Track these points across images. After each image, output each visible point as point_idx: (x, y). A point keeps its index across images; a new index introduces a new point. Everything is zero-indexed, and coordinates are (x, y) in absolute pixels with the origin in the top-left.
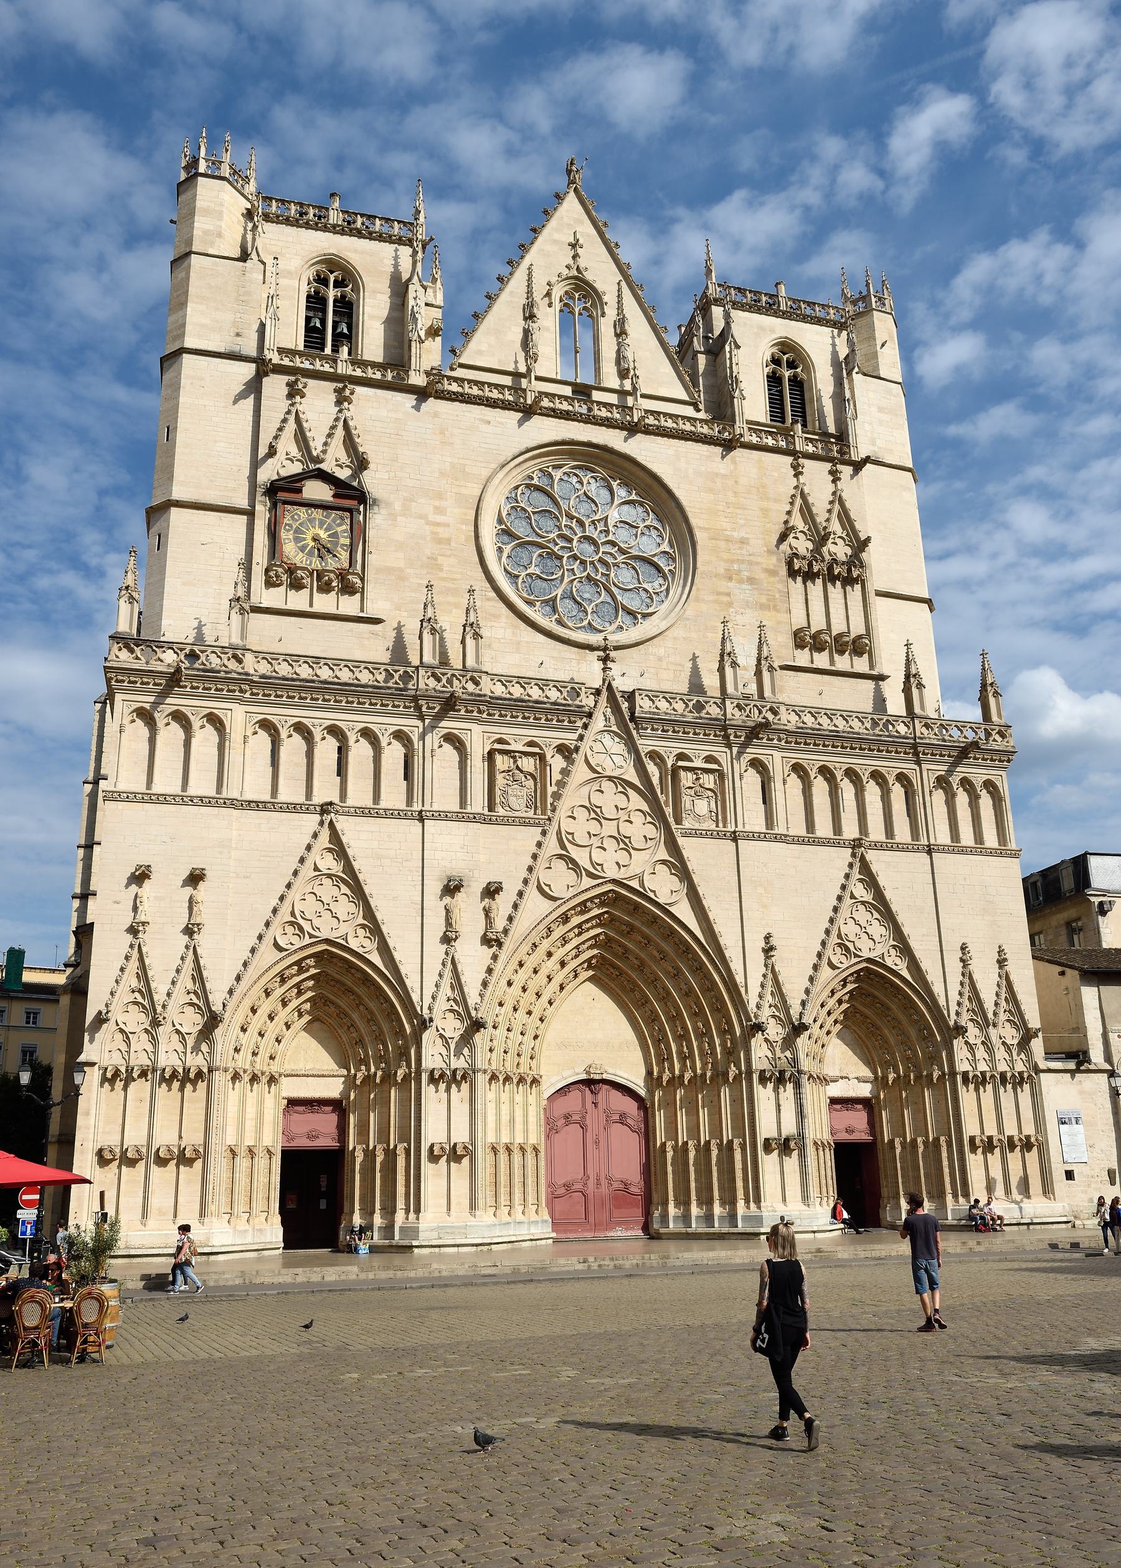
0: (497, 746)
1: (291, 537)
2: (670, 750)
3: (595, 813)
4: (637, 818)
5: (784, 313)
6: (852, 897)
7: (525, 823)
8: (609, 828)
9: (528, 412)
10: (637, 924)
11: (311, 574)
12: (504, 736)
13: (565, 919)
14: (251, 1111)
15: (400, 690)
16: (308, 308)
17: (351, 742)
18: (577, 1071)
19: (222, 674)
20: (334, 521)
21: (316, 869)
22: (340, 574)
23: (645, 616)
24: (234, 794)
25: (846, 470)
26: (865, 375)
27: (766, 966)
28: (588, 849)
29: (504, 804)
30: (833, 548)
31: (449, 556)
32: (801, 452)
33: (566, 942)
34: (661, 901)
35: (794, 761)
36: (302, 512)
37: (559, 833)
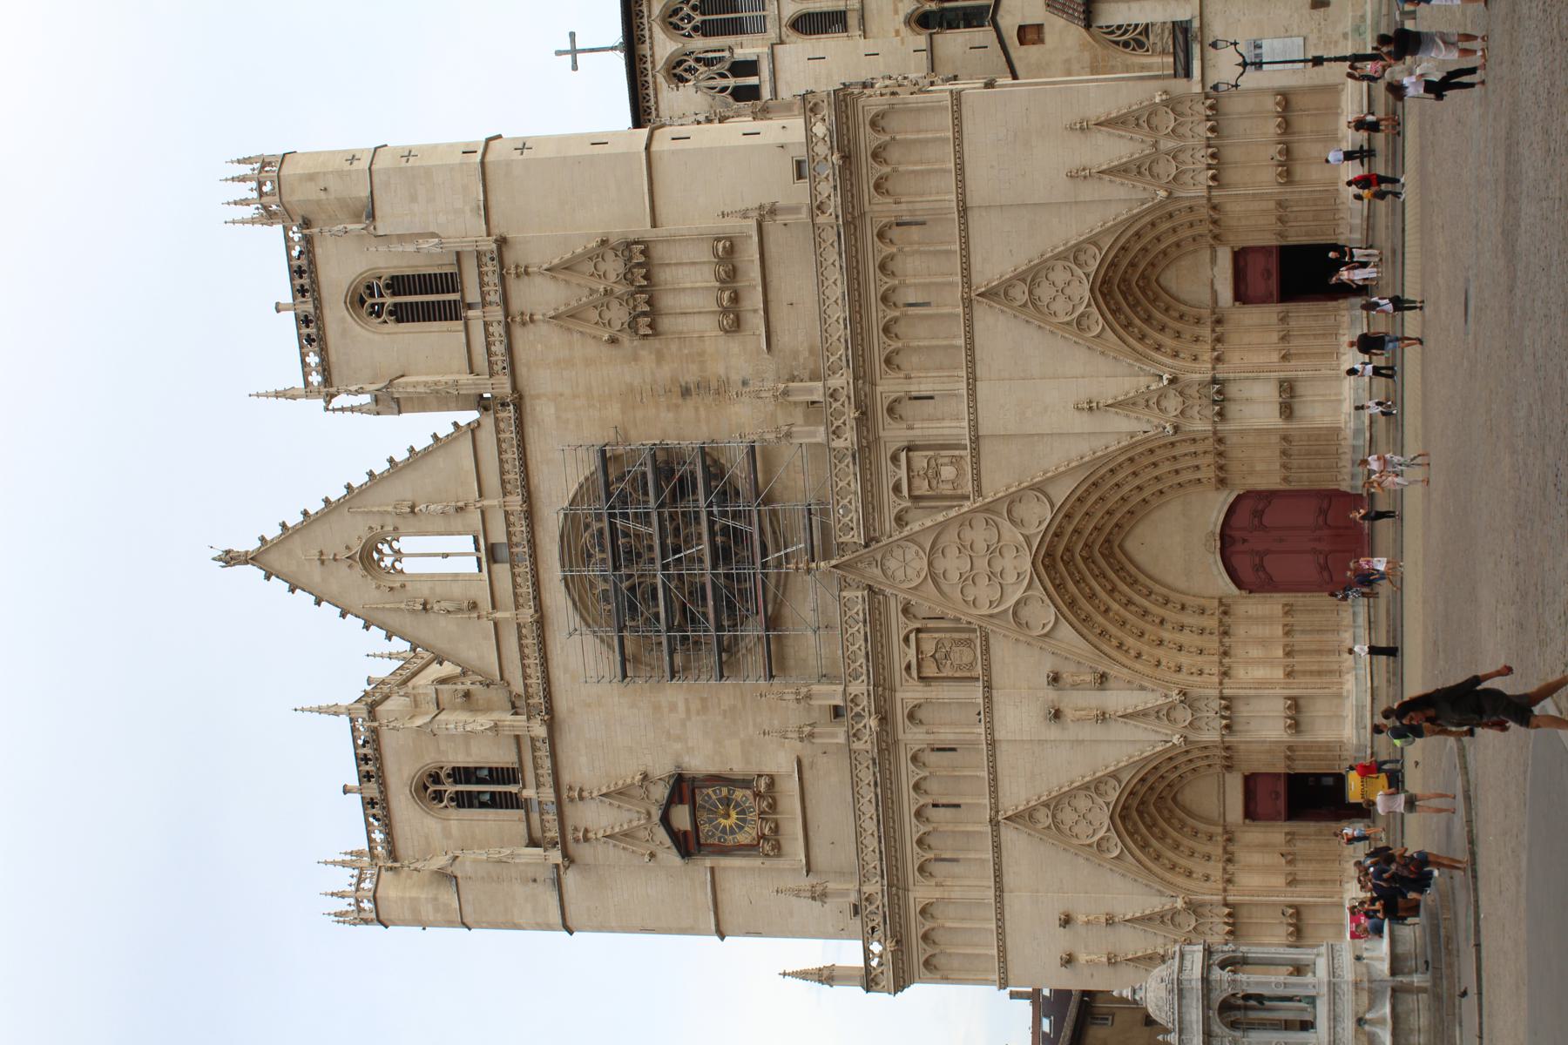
0: (914, 673)
1: (731, 837)
2: (891, 505)
3: (970, 579)
4: (968, 535)
5: (316, 308)
6: (1025, 305)
7: (986, 650)
8: (982, 564)
9: (541, 622)
10: (1071, 528)
11: (763, 819)
12: (903, 666)
13: (1072, 604)
14: (1256, 858)
15: (874, 763)
16: (471, 806)
17: (929, 800)
18: (1211, 561)
19: (886, 909)
20: (706, 802)
21: (1049, 827)
22: (758, 795)
24: (991, 894)
25: (511, 257)
26: (372, 216)
27: (1106, 411)
28: (1004, 587)
29: (971, 665)
30: (612, 277)
31: (719, 699)
32: (506, 316)
33: (1094, 595)
34: (1049, 517)
35: (883, 365)
36: (705, 829)
37: (991, 616)
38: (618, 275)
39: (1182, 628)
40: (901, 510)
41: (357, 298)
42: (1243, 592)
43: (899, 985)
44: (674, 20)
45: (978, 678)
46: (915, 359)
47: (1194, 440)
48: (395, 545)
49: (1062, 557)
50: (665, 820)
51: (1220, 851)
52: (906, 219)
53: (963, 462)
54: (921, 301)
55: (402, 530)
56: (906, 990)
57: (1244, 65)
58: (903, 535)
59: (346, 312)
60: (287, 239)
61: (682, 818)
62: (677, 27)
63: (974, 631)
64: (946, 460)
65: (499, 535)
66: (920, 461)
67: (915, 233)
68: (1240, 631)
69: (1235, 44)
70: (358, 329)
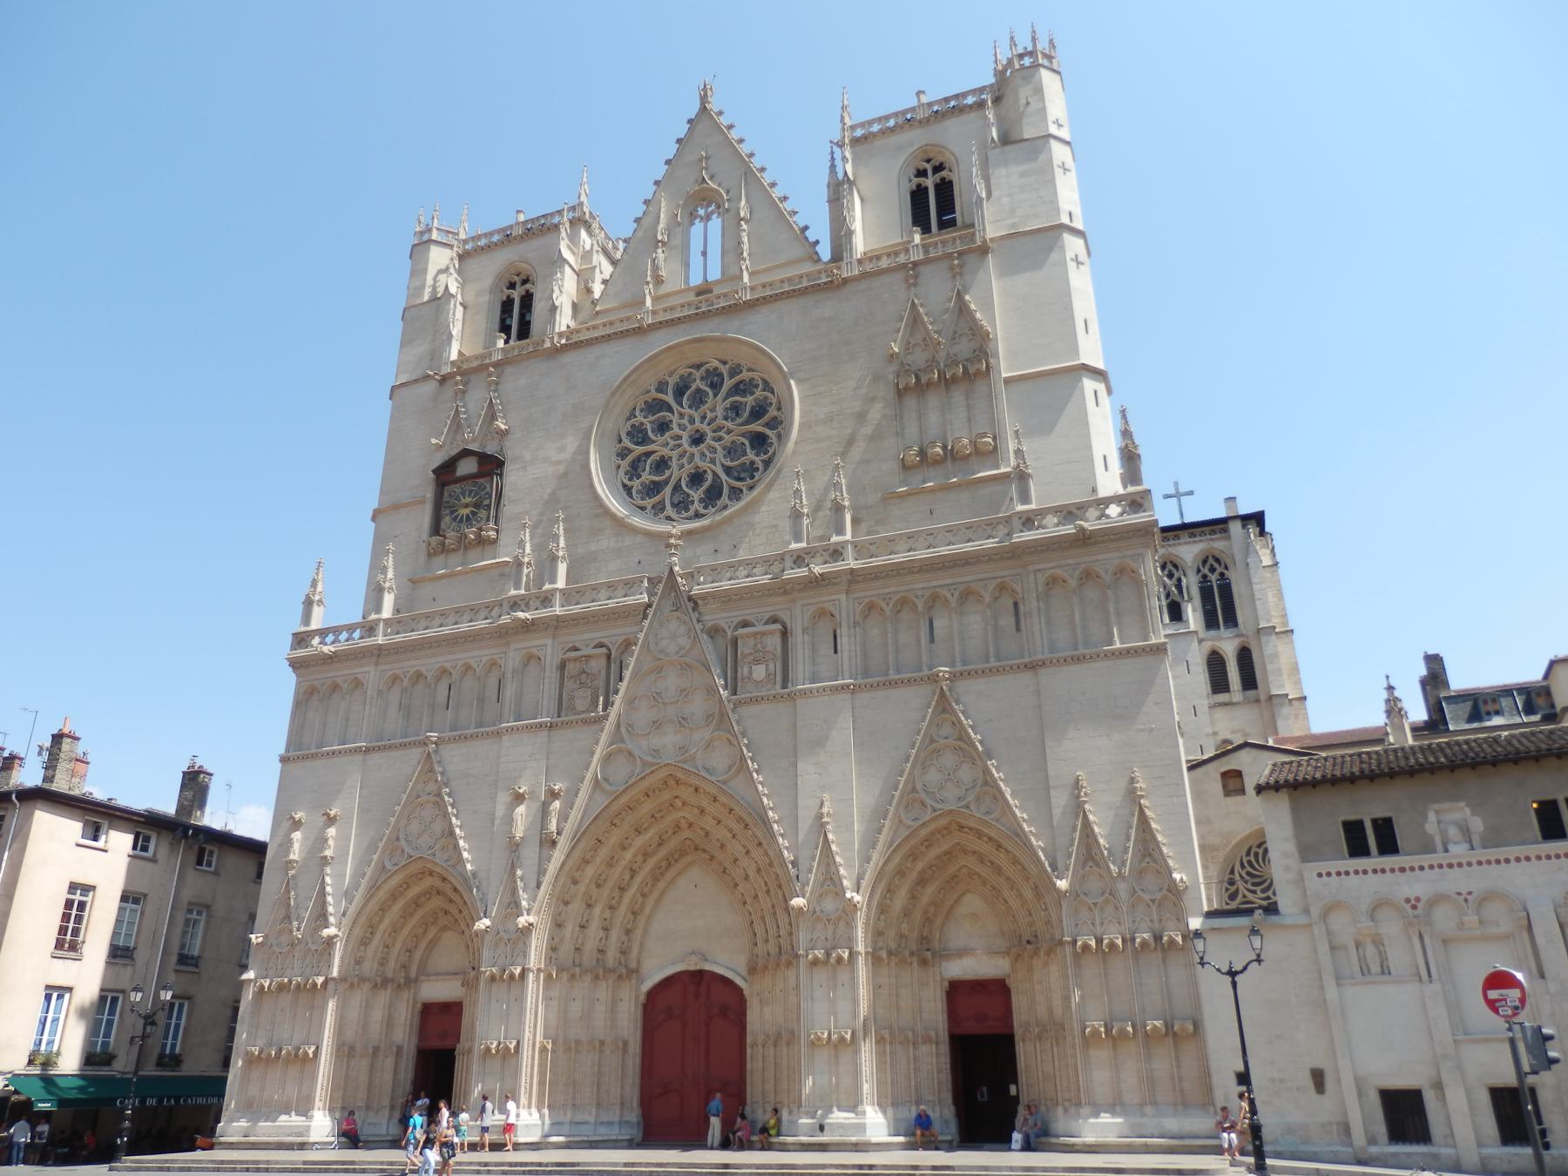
9: (640, 331)
14: (378, 1015)
23: (751, 488)
33: (640, 833)
34: (713, 779)
36: (457, 488)
38: (955, 355)
39: (606, 929)
40: (724, 631)
41: (931, 155)
42: (642, 998)
43: (295, 664)
44: (1211, 561)
45: (559, 716)
46: (875, 632)
47: (791, 934)
48: (715, 215)
49: (677, 797)
50: (466, 453)
51: (390, 975)
52: (1022, 608)
53: (769, 686)
54: (936, 632)
55: (726, 216)
56: (291, 669)
57: (1232, 974)
58: (699, 632)
59: (915, 148)
60: (981, 90)
61: (467, 467)
62: (1205, 562)
63: (605, 709)
64: (771, 667)
65: (717, 291)
66: (774, 642)
67: (1007, 621)
68: (603, 992)
69: (1259, 960)
70: (903, 158)
